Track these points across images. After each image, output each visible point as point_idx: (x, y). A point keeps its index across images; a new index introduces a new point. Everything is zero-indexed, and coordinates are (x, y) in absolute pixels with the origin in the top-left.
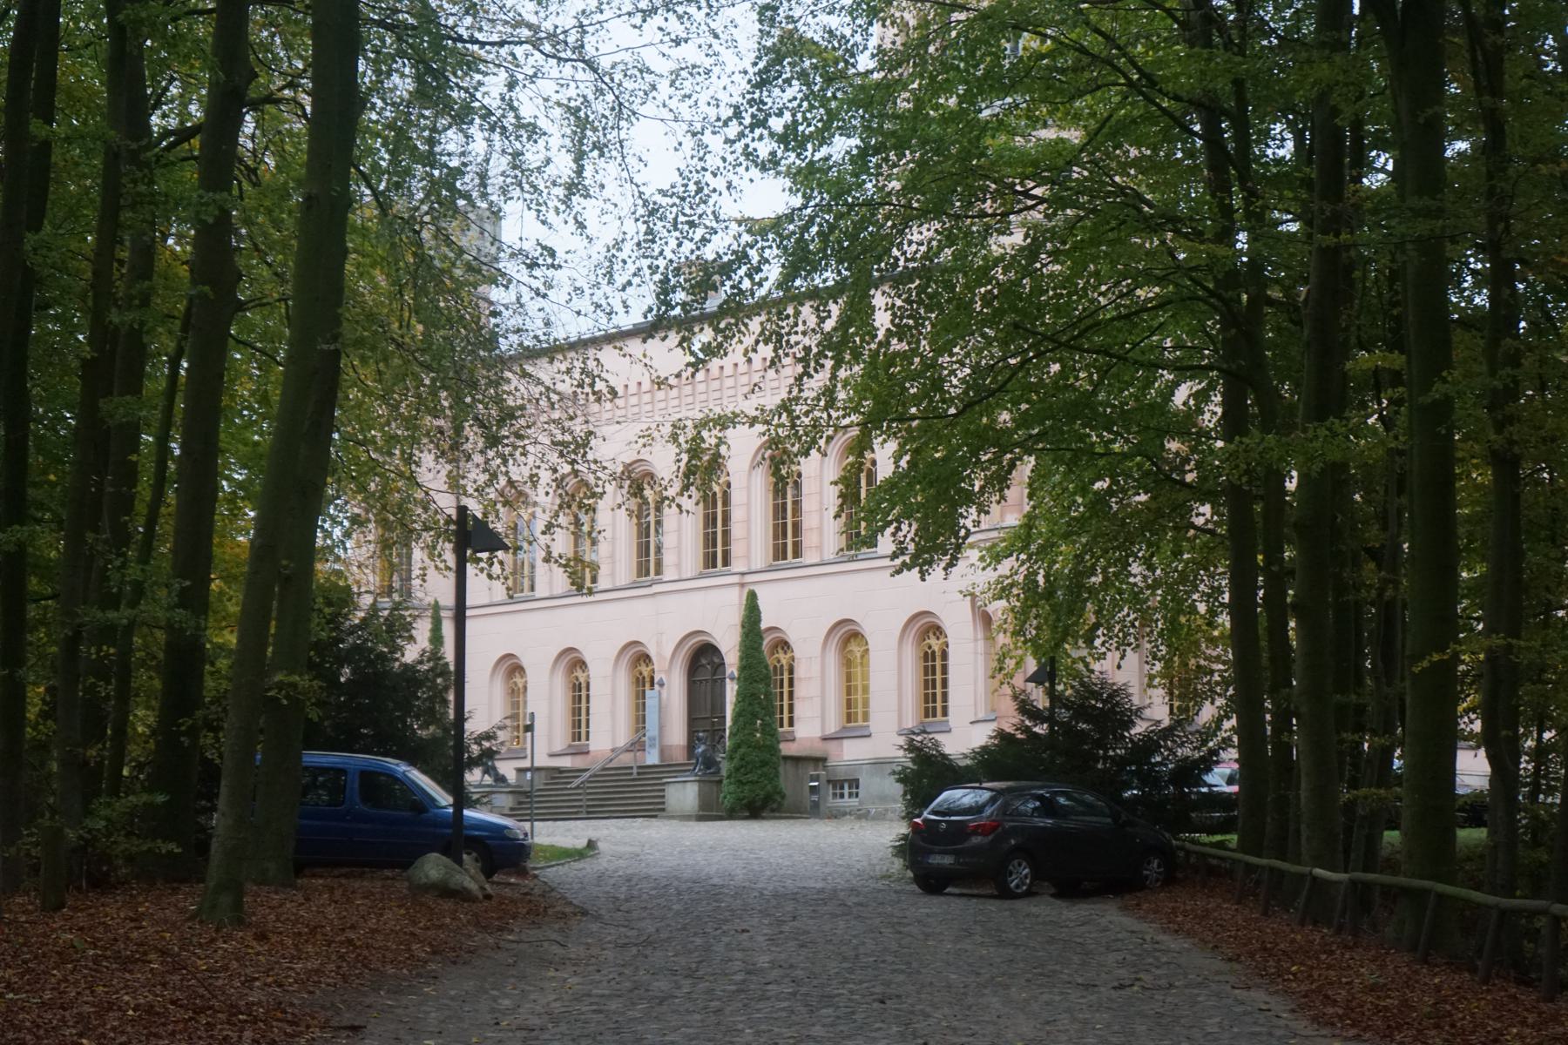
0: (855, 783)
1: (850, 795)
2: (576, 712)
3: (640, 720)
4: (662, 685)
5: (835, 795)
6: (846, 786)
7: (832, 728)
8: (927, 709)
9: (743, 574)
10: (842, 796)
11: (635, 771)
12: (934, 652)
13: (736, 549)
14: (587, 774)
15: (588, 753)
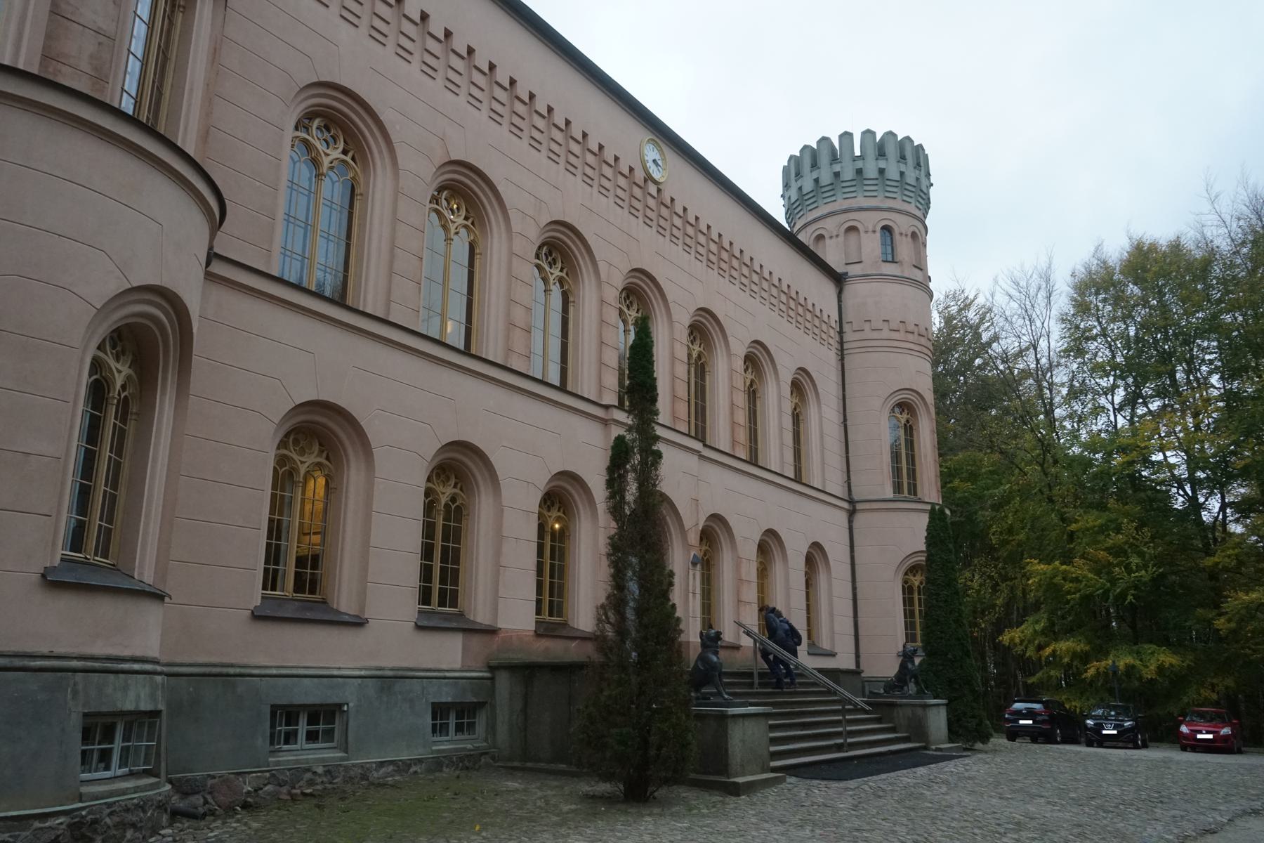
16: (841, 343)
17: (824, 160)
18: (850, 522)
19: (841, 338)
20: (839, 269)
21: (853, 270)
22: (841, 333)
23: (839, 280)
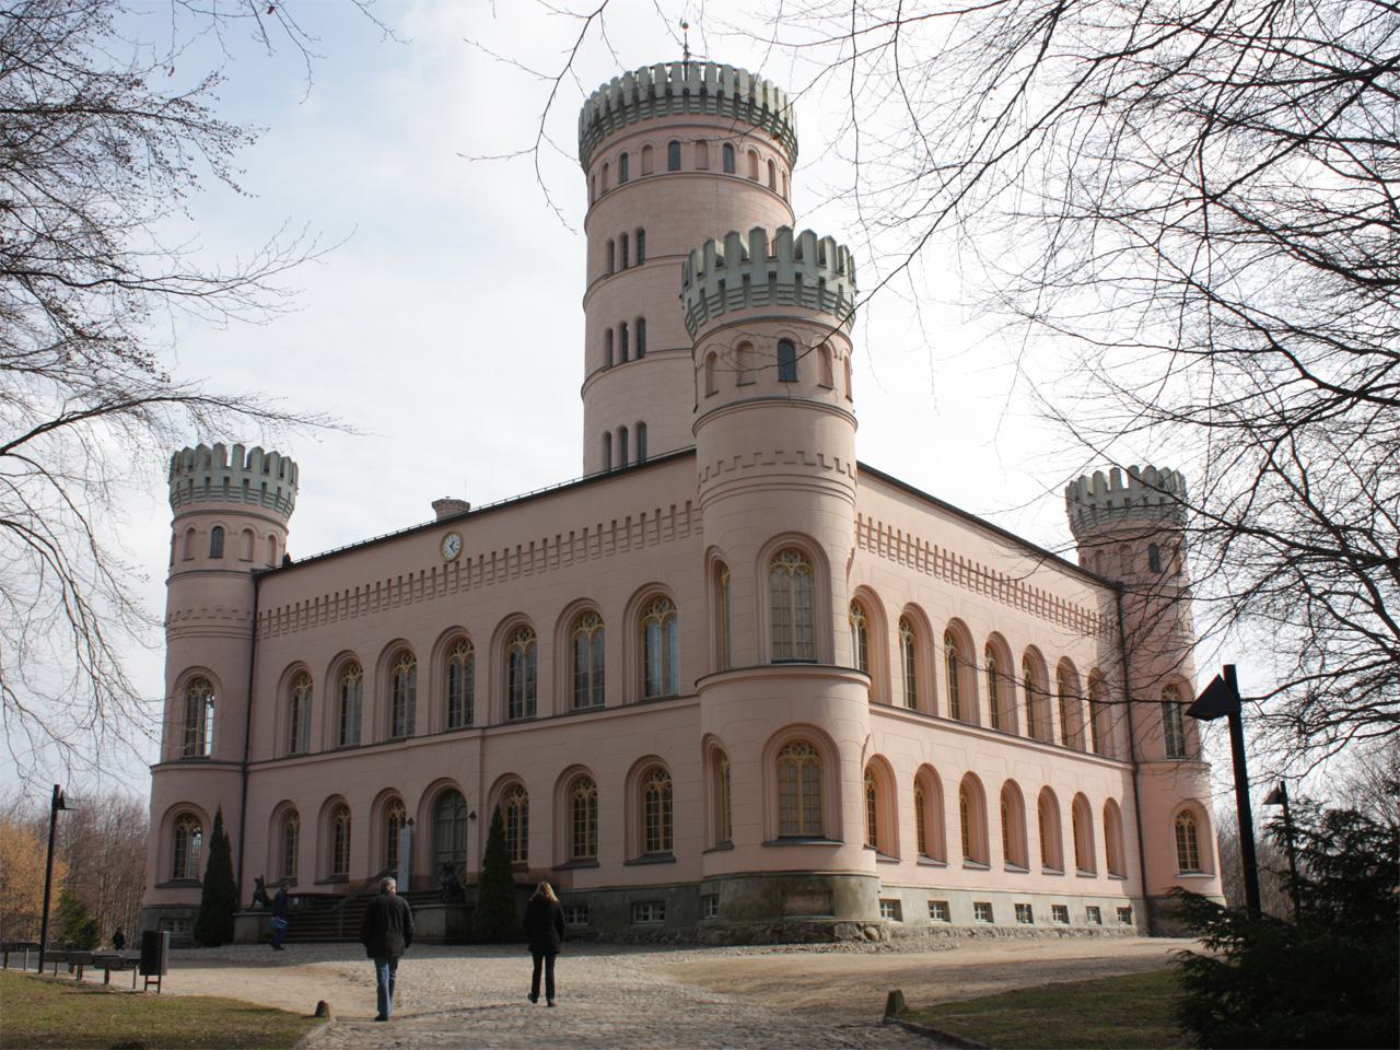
1: (579, 919)
2: (338, 848)
4: (411, 822)
6: (576, 911)
7: (562, 861)
9: (484, 728)
10: (572, 920)
12: (656, 793)
14: (343, 902)
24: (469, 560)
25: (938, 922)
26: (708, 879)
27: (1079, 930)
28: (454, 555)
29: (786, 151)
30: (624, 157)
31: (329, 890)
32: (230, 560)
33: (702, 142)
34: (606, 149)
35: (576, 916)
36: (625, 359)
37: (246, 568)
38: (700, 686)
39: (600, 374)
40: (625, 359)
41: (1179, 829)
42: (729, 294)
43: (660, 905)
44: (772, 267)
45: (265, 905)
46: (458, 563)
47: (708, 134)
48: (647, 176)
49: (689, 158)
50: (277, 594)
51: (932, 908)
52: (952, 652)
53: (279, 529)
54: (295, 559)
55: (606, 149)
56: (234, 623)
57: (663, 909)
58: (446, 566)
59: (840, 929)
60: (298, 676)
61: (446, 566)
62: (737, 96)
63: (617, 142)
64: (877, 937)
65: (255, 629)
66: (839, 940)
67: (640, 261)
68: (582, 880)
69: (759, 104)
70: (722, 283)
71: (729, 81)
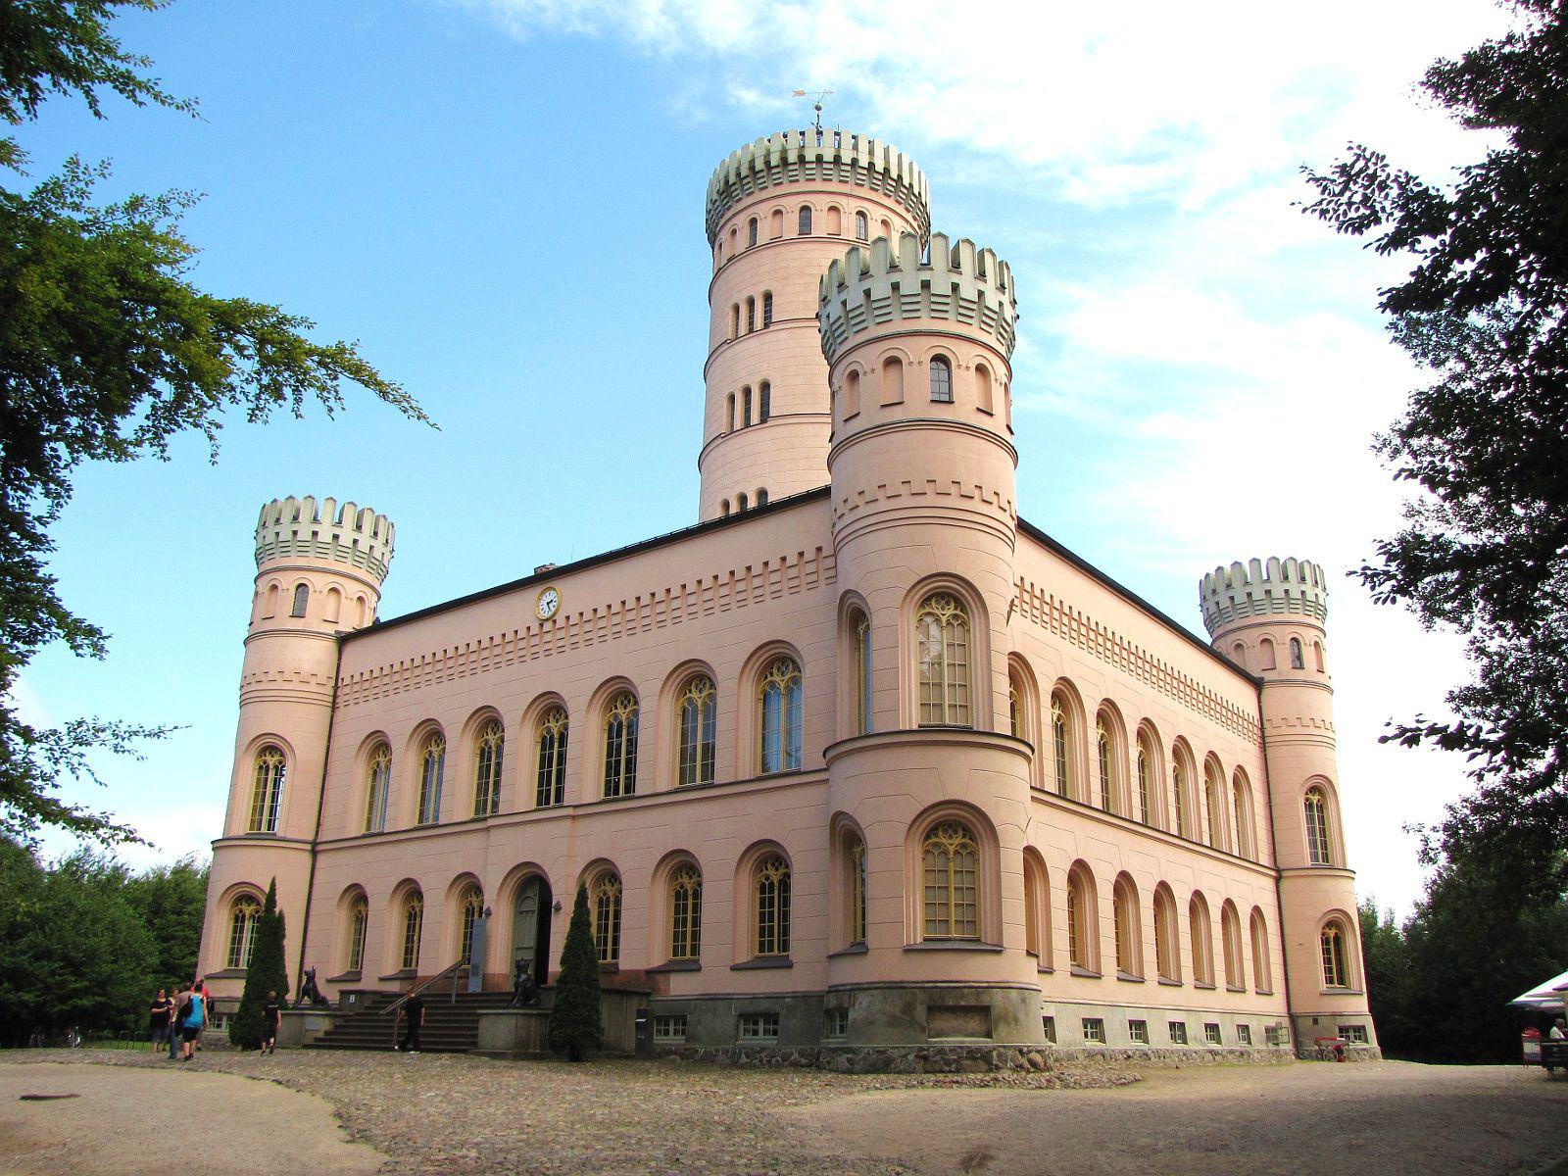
0: (681, 1020)
3: (467, 947)
5: (658, 1031)
6: (672, 1023)
8: (762, 944)
10: (667, 1033)
11: (453, 999)
12: (772, 884)
13: (569, 784)
15: (416, 978)
16: (1263, 737)
17: (1236, 583)
18: (1277, 887)
19: (1263, 732)
20: (1256, 675)
21: (1268, 676)
22: (1262, 729)
23: (1258, 684)
24: (568, 618)
25: (1093, 1044)
26: (834, 990)
27: (1231, 1052)
28: (550, 613)
29: (915, 219)
30: (753, 222)
31: (394, 987)
32: (312, 622)
33: (833, 209)
34: (734, 215)
35: (672, 1028)
36: (747, 424)
37: (331, 629)
38: (830, 755)
39: (720, 440)
40: (747, 424)
41: (1325, 941)
42: (875, 305)
43: (772, 1018)
44: (925, 276)
45: (315, 1002)
46: (555, 621)
47: (842, 202)
48: (776, 241)
49: (821, 224)
50: (362, 658)
51: (1085, 1027)
52: (1102, 736)
53: (369, 591)
54: (383, 620)
55: (734, 215)
56: (312, 687)
57: (776, 1023)
58: (541, 625)
59: (1000, 1055)
60: (379, 746)
61: (541, 625)
62: (871, 165)
63: (745, 208)
64: (1042, 1065)
65: (335, 697)
66: (998, 1068)
67: (766, 326)
68: (680, 986)
69: (894, 174)
70: (867, 293)
71: (863, 147)
